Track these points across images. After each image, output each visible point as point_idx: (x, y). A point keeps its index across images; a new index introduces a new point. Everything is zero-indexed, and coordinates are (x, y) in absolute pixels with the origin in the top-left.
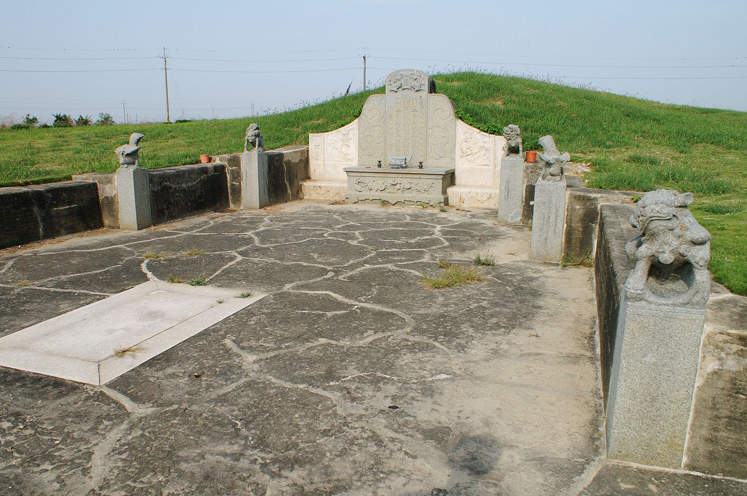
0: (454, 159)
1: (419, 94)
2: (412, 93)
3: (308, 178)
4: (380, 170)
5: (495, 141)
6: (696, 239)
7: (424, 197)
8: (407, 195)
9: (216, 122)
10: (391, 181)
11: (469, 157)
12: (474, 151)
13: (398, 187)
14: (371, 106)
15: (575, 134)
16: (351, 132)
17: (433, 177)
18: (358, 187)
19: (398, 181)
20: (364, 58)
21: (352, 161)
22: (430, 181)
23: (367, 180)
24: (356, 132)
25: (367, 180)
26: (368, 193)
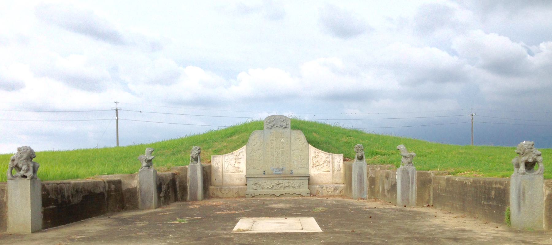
0: (308, 168)
1: (286, 130)
2: (281, 130)
3: (211, 185)
4: (264, 176)
5: (332, 157)
6: (471, 180)
7: (297, 191)
8: (287, 190)
9: (338, 128)
10: (276, 182)
11: (317, 167)
12: (321, 163)
13: (281, 185)
14: (255, 139)
15: (72, 195)
16: (241, 154)
17: (303, 178)
18: (254, 187)
19: (280, 182)
20: (117, 110)
21: (242, 172)
22: (301, 181)
23: (260, 182)
24: (244, 153)
25: (260, 182)
26: (261, 190)
